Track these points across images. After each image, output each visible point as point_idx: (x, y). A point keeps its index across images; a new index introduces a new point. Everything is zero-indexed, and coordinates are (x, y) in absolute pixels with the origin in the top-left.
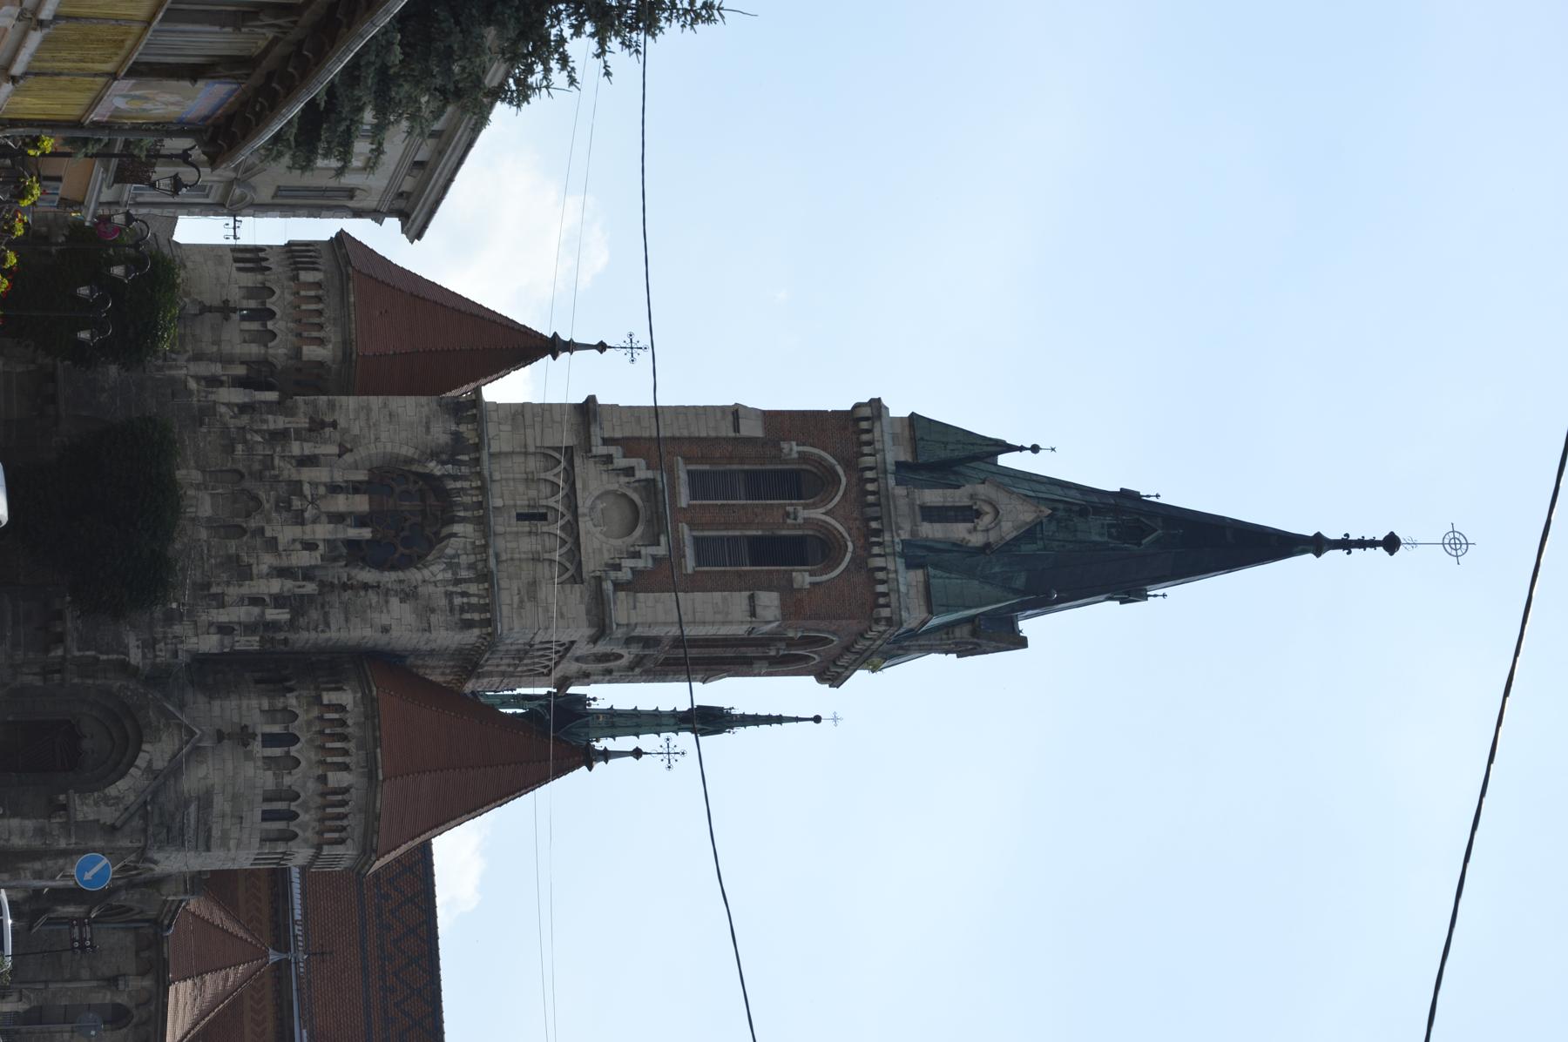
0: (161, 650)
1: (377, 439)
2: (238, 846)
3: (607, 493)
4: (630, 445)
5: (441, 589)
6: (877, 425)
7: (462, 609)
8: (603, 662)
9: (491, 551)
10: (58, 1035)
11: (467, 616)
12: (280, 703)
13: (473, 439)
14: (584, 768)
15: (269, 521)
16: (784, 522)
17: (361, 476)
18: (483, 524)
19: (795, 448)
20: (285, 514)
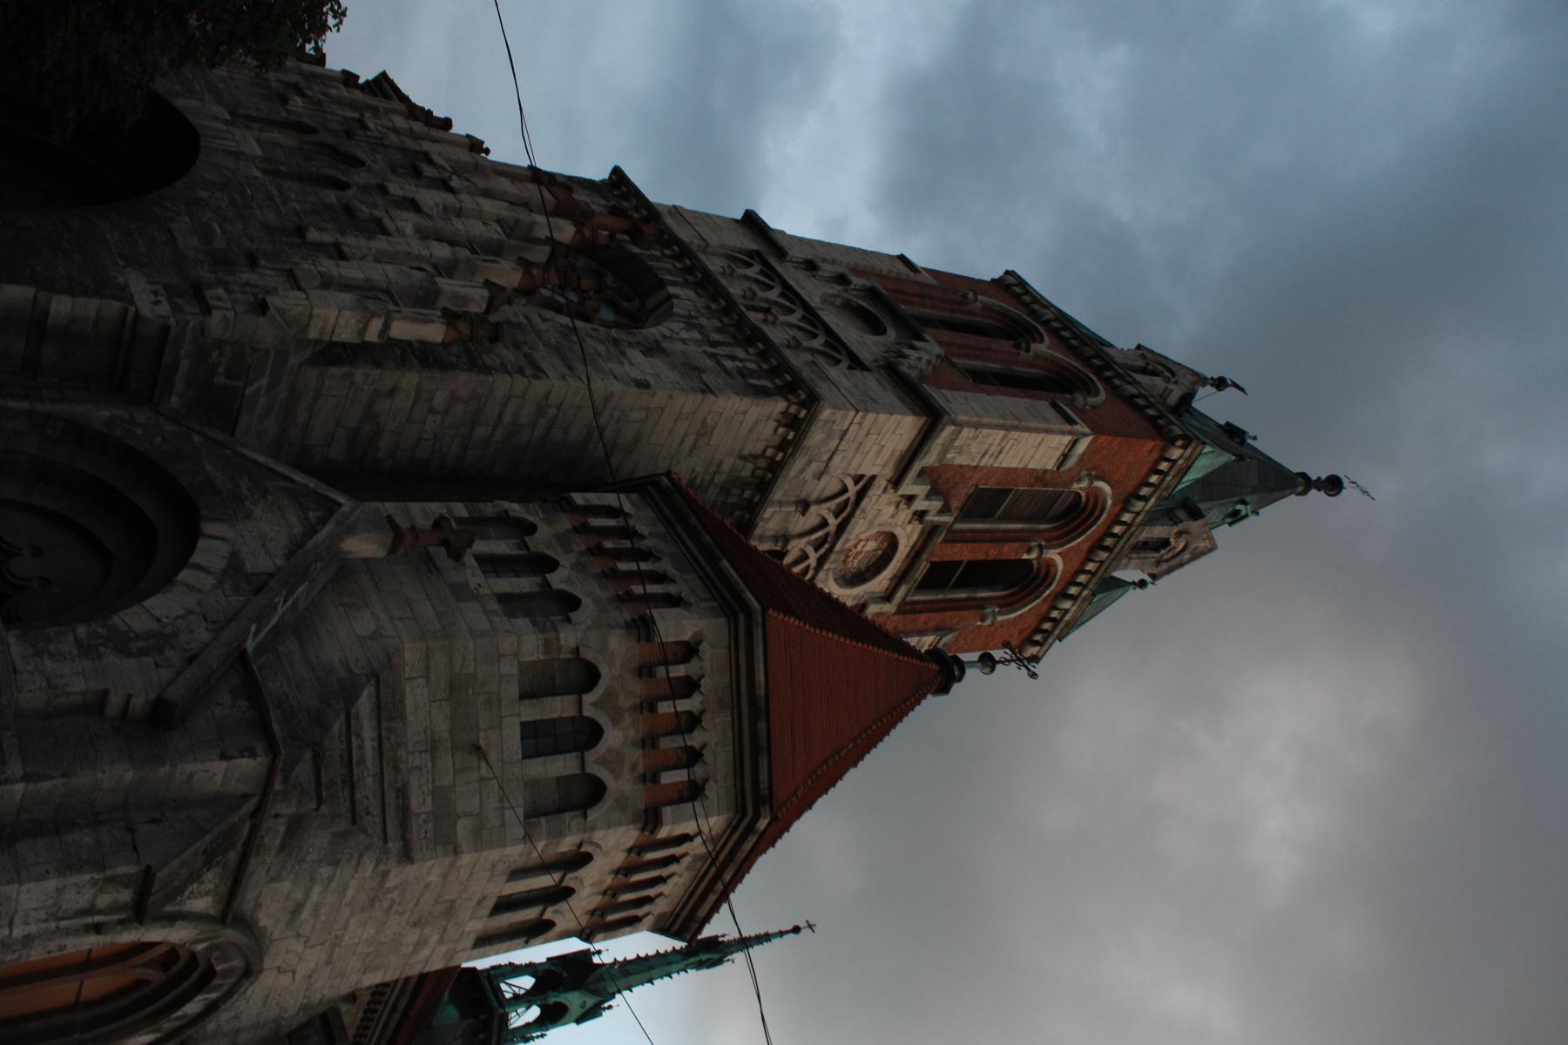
0: (220, 299)
12: (488, 509)
14: (929, 697)
16: (1019, 354)
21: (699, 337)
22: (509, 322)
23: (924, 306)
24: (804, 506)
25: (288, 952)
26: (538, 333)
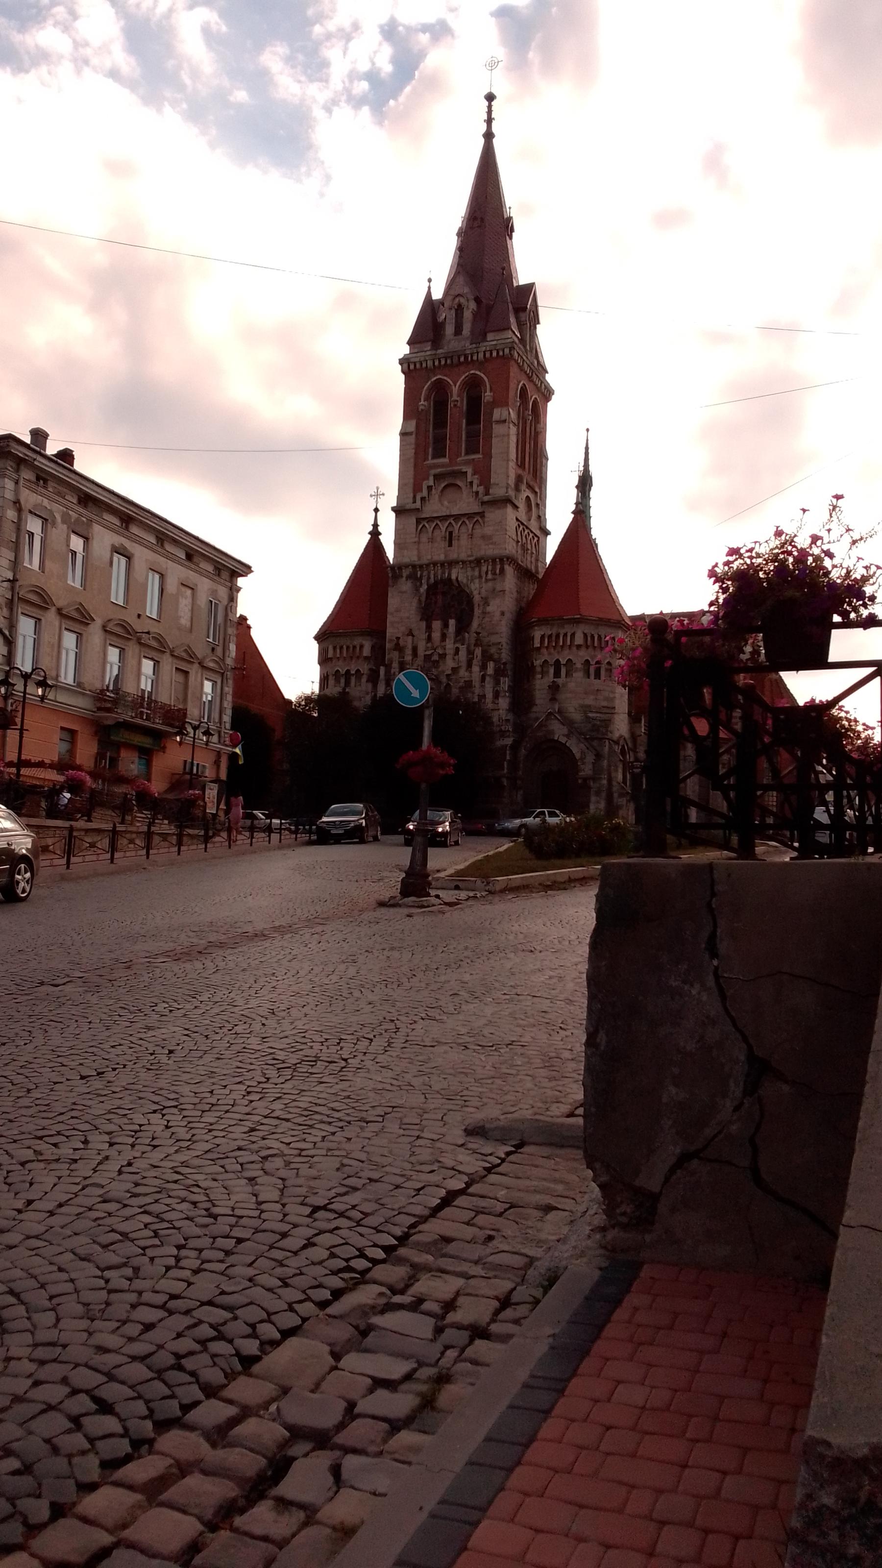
1: (408, 618)
3: (440, 501)
4: (417, 488)
5: (484, 585)
6: (412, 360)
7: (494, 574)
9: (465, 559)
11: (498, 571)
12: (539, 669)
13: (410, 569)
15: (444, 672)
17: (423, 624)
18: (452, 564)
19: (422, 402)
20: (441, 664)
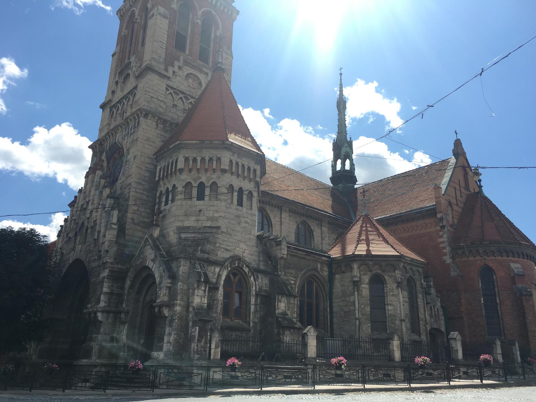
2: (217, 211)
7: (134, 128)
8: (202, 84)
10: (390, 312)
21: (126, 137)
22: (121, 188)
23: (126, 51)
24: (175, 106)
25: (239, 251)
26: (123, 182)
